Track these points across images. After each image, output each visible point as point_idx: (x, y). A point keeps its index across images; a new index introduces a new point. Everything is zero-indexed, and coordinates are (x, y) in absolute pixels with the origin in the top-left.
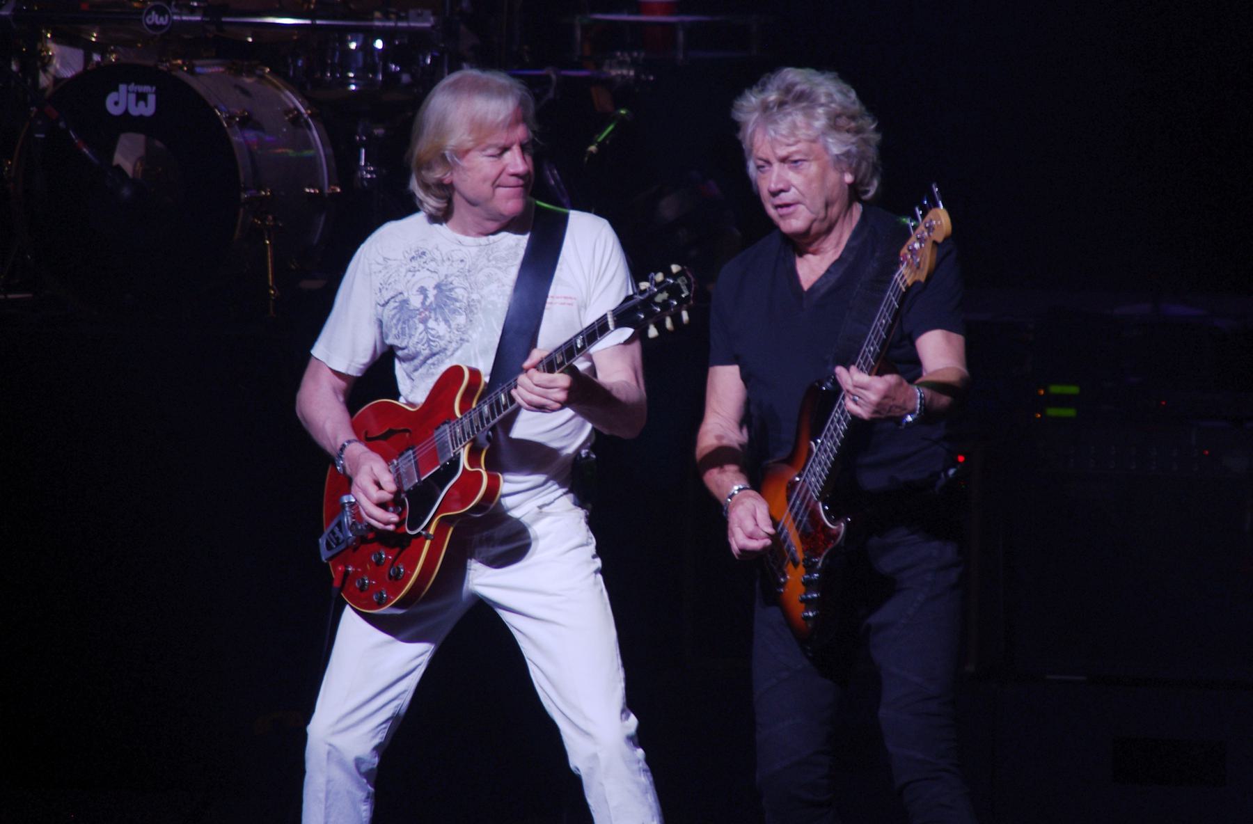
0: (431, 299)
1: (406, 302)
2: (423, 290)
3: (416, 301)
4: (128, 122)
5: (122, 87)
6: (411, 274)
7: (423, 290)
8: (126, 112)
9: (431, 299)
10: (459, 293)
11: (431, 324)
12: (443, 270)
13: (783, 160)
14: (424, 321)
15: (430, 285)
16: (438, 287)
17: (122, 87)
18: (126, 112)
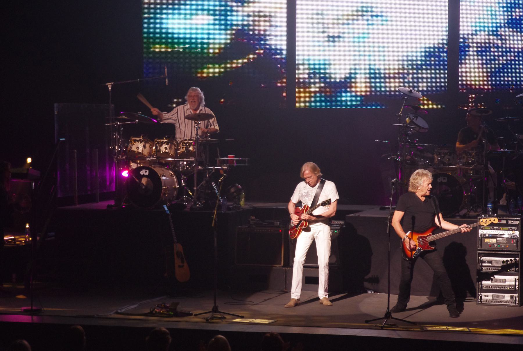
0: (306, 194)
1: (302, 194)
2: (305, 193)
3: (304, 194)
4: (144, 176)
5: (143, 170)
6: (303, 190)
7: (305, 193)
8: (144, 174)
9: (306, 194)
10: (310, 194)
11: (306, 198)
12: (308, 190)
13: (308, 178)
14: (305, 197)
15: (306, 192)
16: (307, 192)
17: (143, 170)
18: (144, 174)
